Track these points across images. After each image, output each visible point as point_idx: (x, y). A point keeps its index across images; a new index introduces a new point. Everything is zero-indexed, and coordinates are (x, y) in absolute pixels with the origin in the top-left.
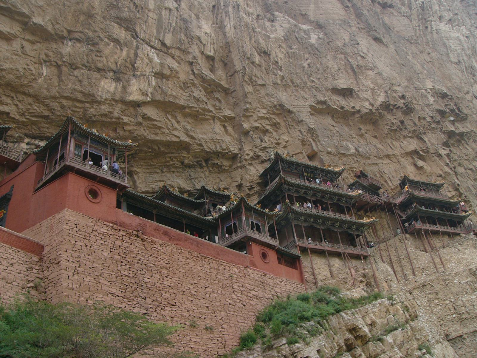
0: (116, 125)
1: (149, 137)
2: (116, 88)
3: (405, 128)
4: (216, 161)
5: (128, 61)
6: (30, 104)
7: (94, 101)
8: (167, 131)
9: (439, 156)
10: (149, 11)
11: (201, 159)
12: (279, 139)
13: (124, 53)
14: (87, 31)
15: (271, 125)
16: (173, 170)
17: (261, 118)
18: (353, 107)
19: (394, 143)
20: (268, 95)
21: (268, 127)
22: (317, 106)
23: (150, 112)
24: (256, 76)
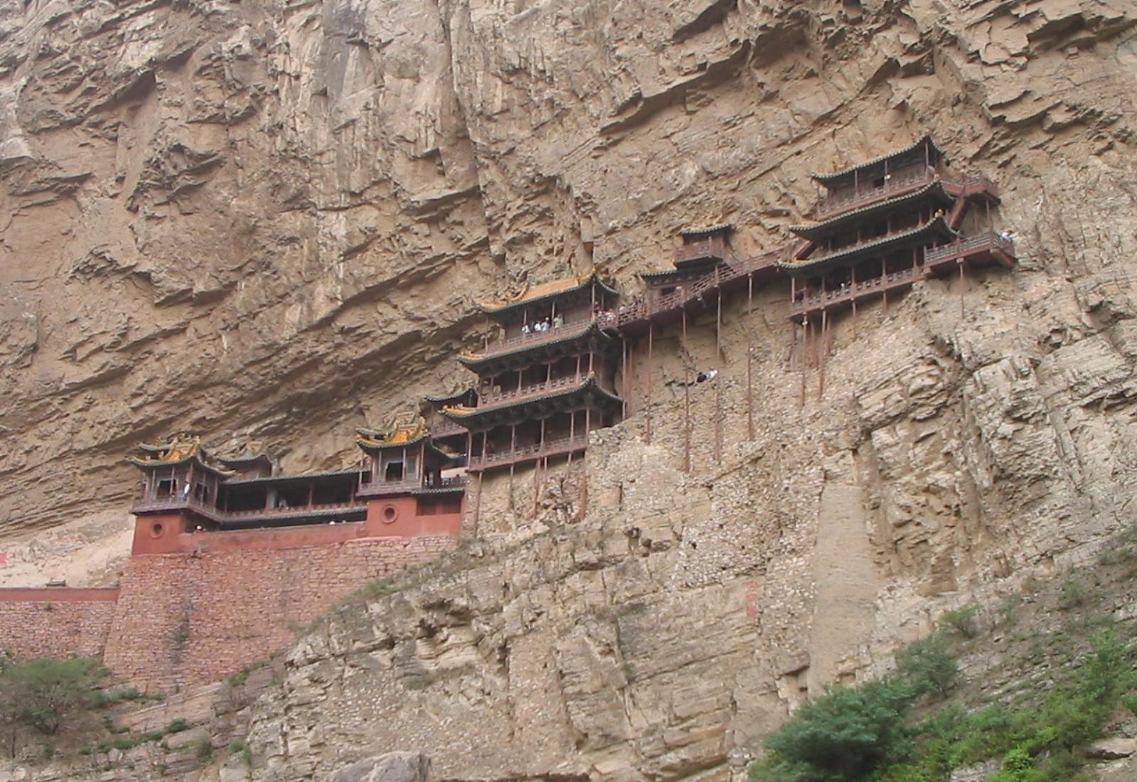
0: (315, 362)
1: (357, 357)
2: (302, 313)
3: (865, 12)
4: (471, 333)
5: (313, 257)
6: (222, 394)
7: (279, 350)
8: (380, 332)
9: (954, 41)
10: (321, 154)
11: (448, 342)
12: (551, 241)
13: (305, 248)
14: (256, 253)
15: (537, 220)
16: (415, 377)
17: (516, 218)
18: (735, 43)
19: (845, 70)
20: (519, 166)
21: (531, 229)
22: (620, 119)
23: (347, 321)
24: (497, 141)
